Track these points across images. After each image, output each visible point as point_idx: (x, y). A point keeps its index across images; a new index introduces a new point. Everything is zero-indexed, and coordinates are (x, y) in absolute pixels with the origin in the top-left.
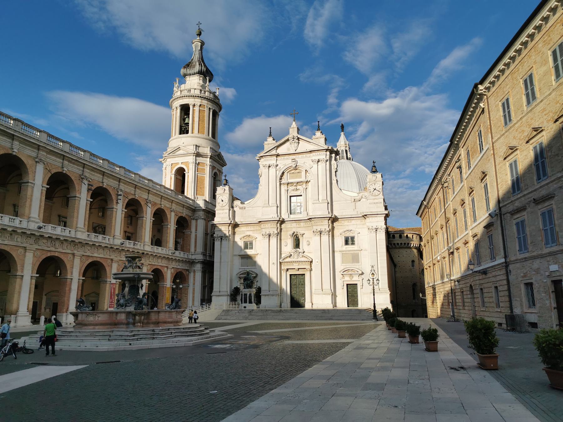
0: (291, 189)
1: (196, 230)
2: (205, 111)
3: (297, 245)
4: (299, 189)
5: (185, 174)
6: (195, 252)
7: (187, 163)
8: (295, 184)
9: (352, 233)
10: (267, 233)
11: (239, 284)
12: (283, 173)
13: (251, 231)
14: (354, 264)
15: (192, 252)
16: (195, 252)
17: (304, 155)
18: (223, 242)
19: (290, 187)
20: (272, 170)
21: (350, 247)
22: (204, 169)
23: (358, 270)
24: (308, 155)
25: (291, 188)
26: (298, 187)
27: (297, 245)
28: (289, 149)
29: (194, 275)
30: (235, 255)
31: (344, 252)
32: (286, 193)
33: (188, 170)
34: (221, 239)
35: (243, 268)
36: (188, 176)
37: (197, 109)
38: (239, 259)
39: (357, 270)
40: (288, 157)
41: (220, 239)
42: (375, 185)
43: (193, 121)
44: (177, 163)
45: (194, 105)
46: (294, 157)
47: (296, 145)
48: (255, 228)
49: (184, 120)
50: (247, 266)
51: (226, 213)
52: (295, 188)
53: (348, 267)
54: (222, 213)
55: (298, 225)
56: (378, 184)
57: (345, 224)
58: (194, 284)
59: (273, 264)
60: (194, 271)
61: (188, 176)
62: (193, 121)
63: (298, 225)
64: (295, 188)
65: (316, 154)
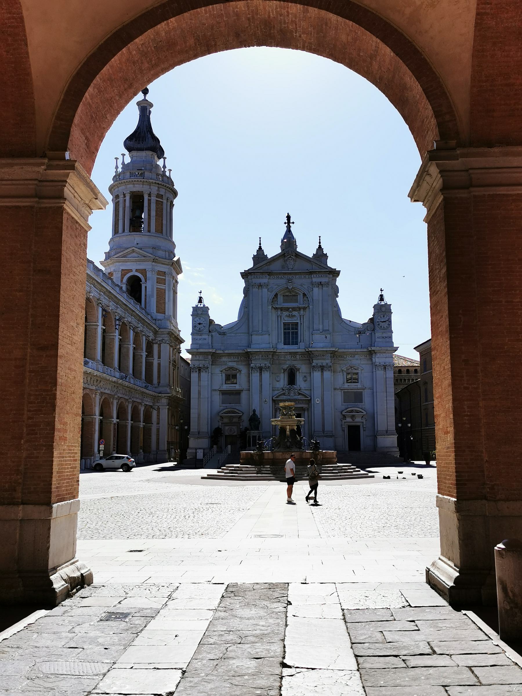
0: (285, 314)
1: (159, 357)
2: (162, 202)
3: (292, 380)
4: (295, 315)
5: (141, 285)
6: (159, 385)
7: (144, 272)
8: (290, 310)
9: (356, 369)
10: (258, 365)
11: (220, 424)
12: (276, 295)
13: (235, 362)
14: (356, 404)
15: (154, 385)
16: (159, 385)
17: (303, 276)
18: (203, 374)
19: (284, 312)
20: (265, 290)
21: (353, 385)
22: (165, 279)
23: (362, 411)
24: (307, 276)
25: (285, 313)
26: (294, 313)
27: (292, 380)
28: (283, 267)
29: (159, 413)
30: (215, 390)
31: (346, 391)
32: (279, 319)
33: (146, 281)
34: (199, 370)
35: (226, 405)
36: (146, 287)
37: (153, 199)
38: (220, 395)
39: (361, 410)
40: (282, 276)
41: (197, 370)
42: (384, 316)
43: (149, 215)
44: (131, 270)
45: (150, 195)
46: (290, 277)
47: (292, 262)
48: (239, 359)
49: (137, 213)
50: (230, 404)
51: (205, 339)
52: (291, 314)
53: (349, 406)
54: (200, 339)
55: (293, 358)
56: (387, 315)
57: (348, 358)
58: (158, 423)
59: (266, 401)
60: (159, 409)
61: (146, 287)
62: (149, 215)
63: (293, 358)
64: (291, 314)
65: (318, 276)
